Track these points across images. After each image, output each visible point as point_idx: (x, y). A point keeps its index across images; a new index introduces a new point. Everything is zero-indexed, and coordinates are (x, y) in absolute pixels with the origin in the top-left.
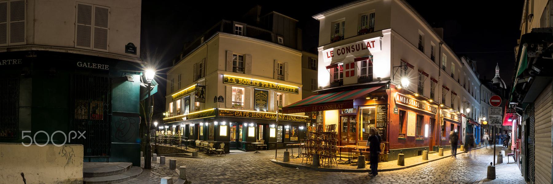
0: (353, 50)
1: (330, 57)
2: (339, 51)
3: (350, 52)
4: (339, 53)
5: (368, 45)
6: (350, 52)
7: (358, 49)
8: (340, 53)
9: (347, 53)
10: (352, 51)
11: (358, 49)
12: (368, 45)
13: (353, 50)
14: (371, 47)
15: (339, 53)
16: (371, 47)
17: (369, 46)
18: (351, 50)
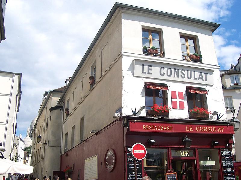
0: (183, 76)
1: (145, 73)
2: (162, 69)
3: (178, 77)
4: (162, 73)
5: (201, 77)
6: (178, 77)
7: (189, 77)
8: (164, 74)
9: (174, 76)
10: (181, 76)
11: (189, 77)
12: (201, 77)
13: (183, 76)
14: (203, 80)
15: (162, 73)
16: (203, 80)
17: (201, 78)
18: (180, 74)
